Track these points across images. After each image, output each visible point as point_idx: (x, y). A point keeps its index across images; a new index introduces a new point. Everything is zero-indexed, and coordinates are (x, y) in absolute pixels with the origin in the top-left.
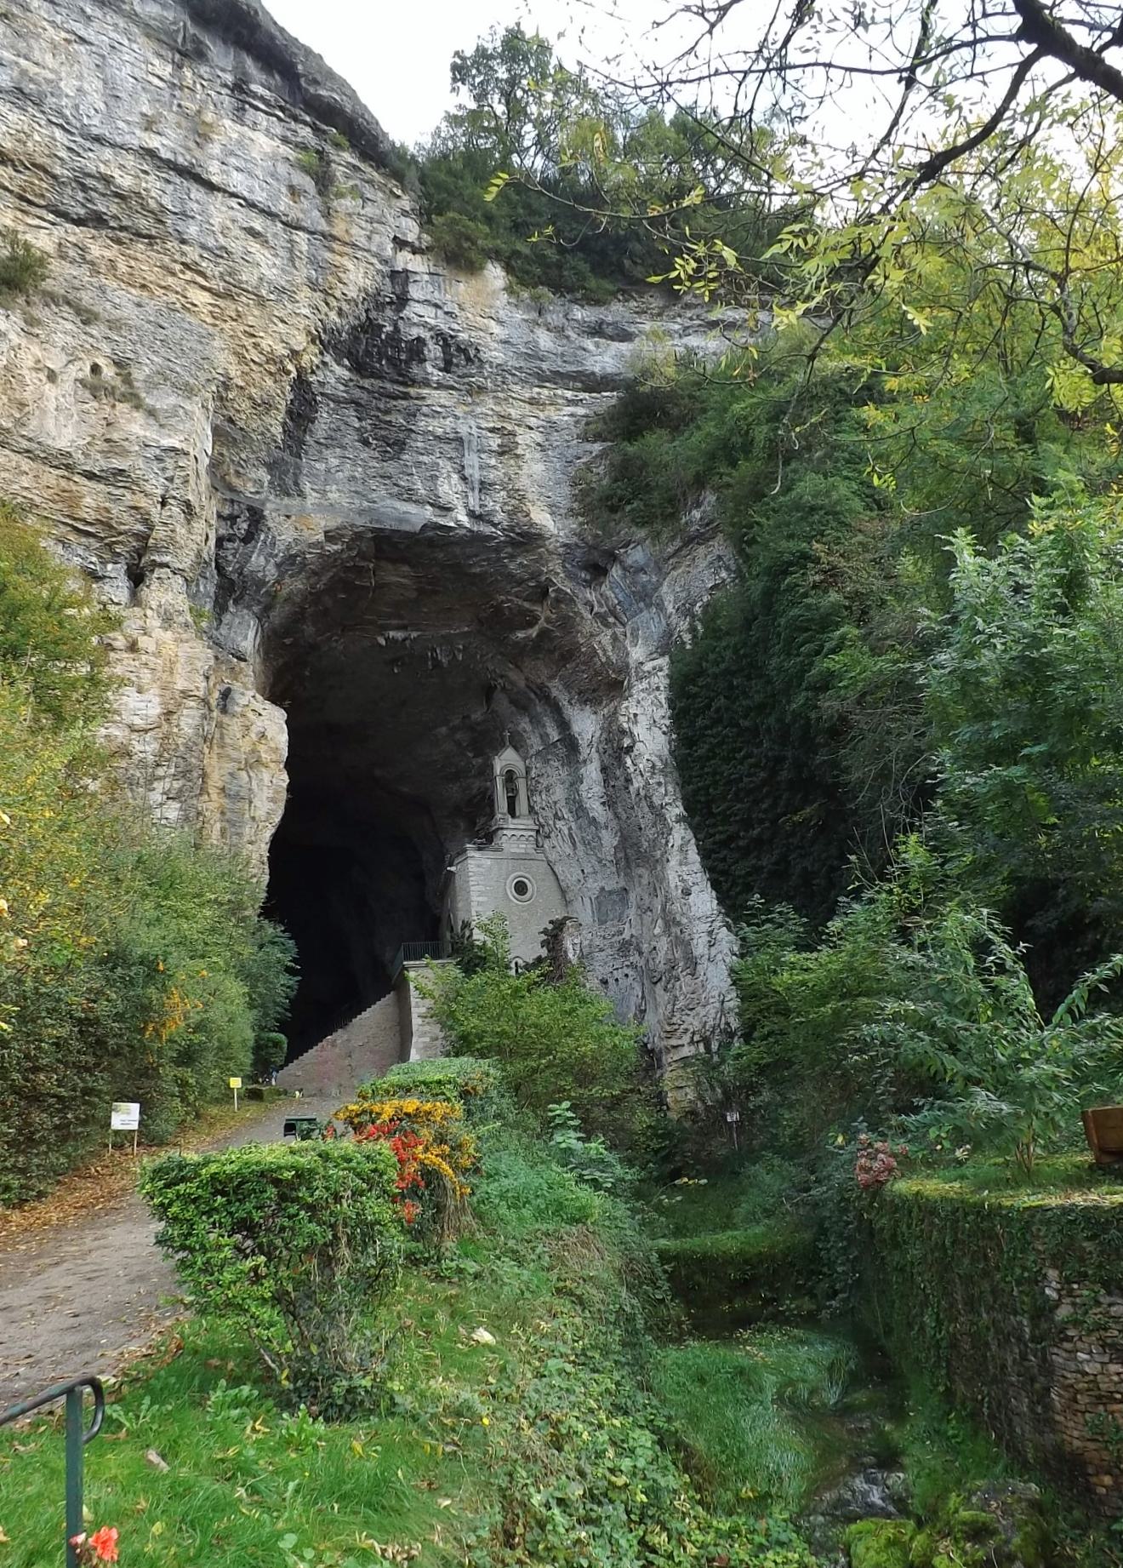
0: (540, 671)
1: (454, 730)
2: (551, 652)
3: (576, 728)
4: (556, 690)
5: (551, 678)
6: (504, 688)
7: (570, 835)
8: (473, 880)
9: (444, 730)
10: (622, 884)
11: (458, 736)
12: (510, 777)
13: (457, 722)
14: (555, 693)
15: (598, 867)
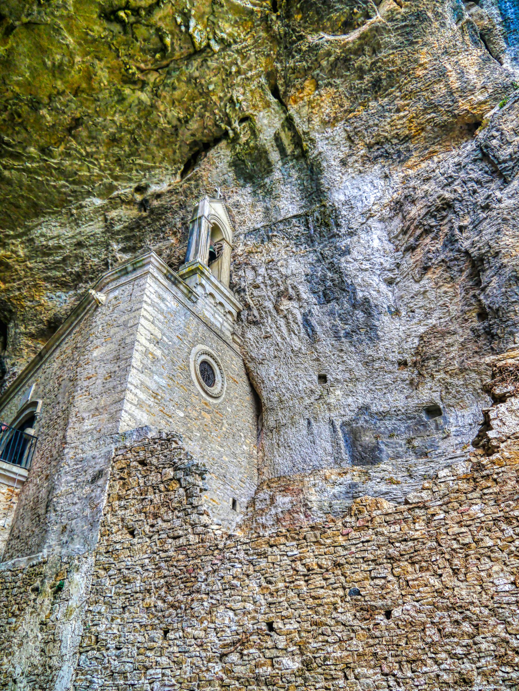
0: (317, 108)
1: (117, 202)
2: (361, 72)
3: (338, 197)
4: (329, 147)
5: (329, 123)
6: (235, 140)
7: (307, 323)
8: (147, 311)
9: (98, 202)
10: (428, 393)
11: (113, 214)
12: (215, 230)
13: (125, 189)
14: (322, 146)
15: (360, 371)
